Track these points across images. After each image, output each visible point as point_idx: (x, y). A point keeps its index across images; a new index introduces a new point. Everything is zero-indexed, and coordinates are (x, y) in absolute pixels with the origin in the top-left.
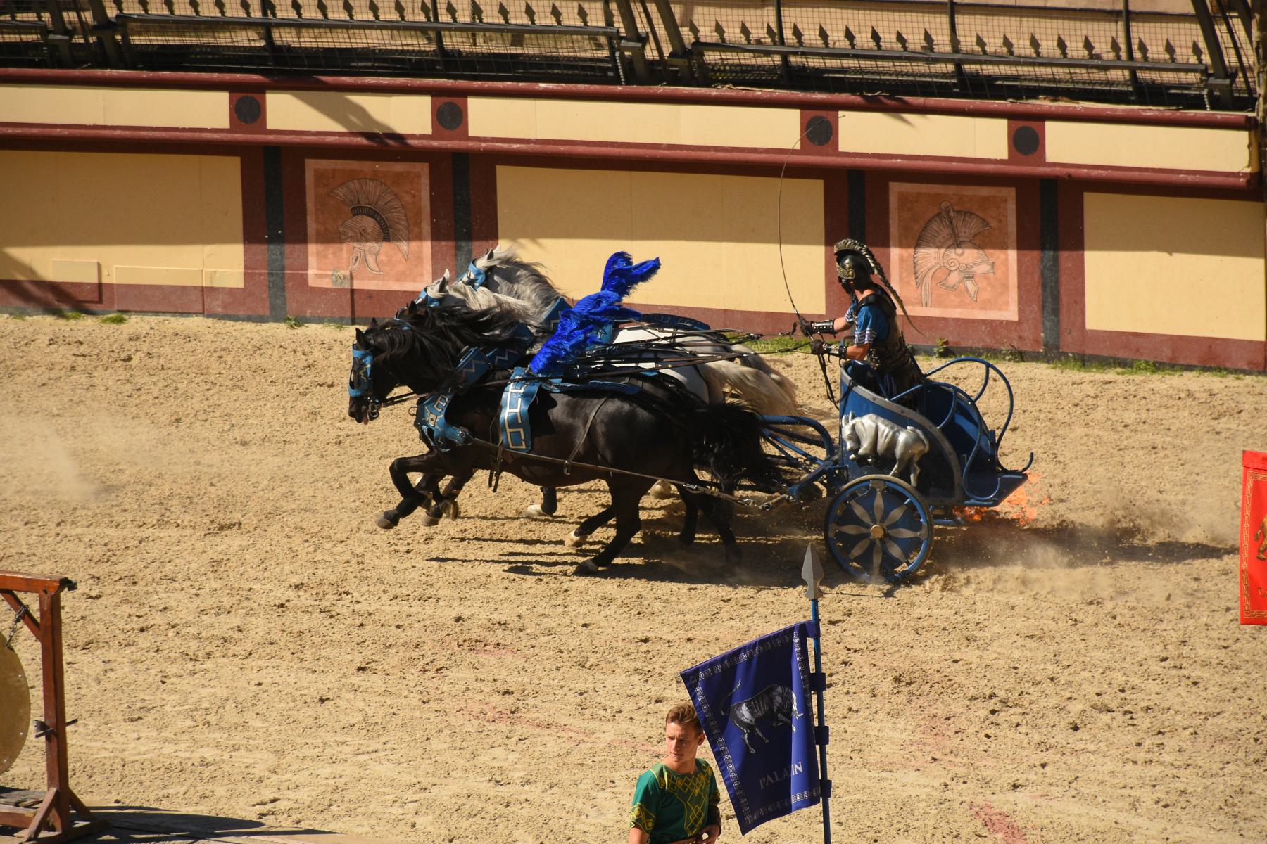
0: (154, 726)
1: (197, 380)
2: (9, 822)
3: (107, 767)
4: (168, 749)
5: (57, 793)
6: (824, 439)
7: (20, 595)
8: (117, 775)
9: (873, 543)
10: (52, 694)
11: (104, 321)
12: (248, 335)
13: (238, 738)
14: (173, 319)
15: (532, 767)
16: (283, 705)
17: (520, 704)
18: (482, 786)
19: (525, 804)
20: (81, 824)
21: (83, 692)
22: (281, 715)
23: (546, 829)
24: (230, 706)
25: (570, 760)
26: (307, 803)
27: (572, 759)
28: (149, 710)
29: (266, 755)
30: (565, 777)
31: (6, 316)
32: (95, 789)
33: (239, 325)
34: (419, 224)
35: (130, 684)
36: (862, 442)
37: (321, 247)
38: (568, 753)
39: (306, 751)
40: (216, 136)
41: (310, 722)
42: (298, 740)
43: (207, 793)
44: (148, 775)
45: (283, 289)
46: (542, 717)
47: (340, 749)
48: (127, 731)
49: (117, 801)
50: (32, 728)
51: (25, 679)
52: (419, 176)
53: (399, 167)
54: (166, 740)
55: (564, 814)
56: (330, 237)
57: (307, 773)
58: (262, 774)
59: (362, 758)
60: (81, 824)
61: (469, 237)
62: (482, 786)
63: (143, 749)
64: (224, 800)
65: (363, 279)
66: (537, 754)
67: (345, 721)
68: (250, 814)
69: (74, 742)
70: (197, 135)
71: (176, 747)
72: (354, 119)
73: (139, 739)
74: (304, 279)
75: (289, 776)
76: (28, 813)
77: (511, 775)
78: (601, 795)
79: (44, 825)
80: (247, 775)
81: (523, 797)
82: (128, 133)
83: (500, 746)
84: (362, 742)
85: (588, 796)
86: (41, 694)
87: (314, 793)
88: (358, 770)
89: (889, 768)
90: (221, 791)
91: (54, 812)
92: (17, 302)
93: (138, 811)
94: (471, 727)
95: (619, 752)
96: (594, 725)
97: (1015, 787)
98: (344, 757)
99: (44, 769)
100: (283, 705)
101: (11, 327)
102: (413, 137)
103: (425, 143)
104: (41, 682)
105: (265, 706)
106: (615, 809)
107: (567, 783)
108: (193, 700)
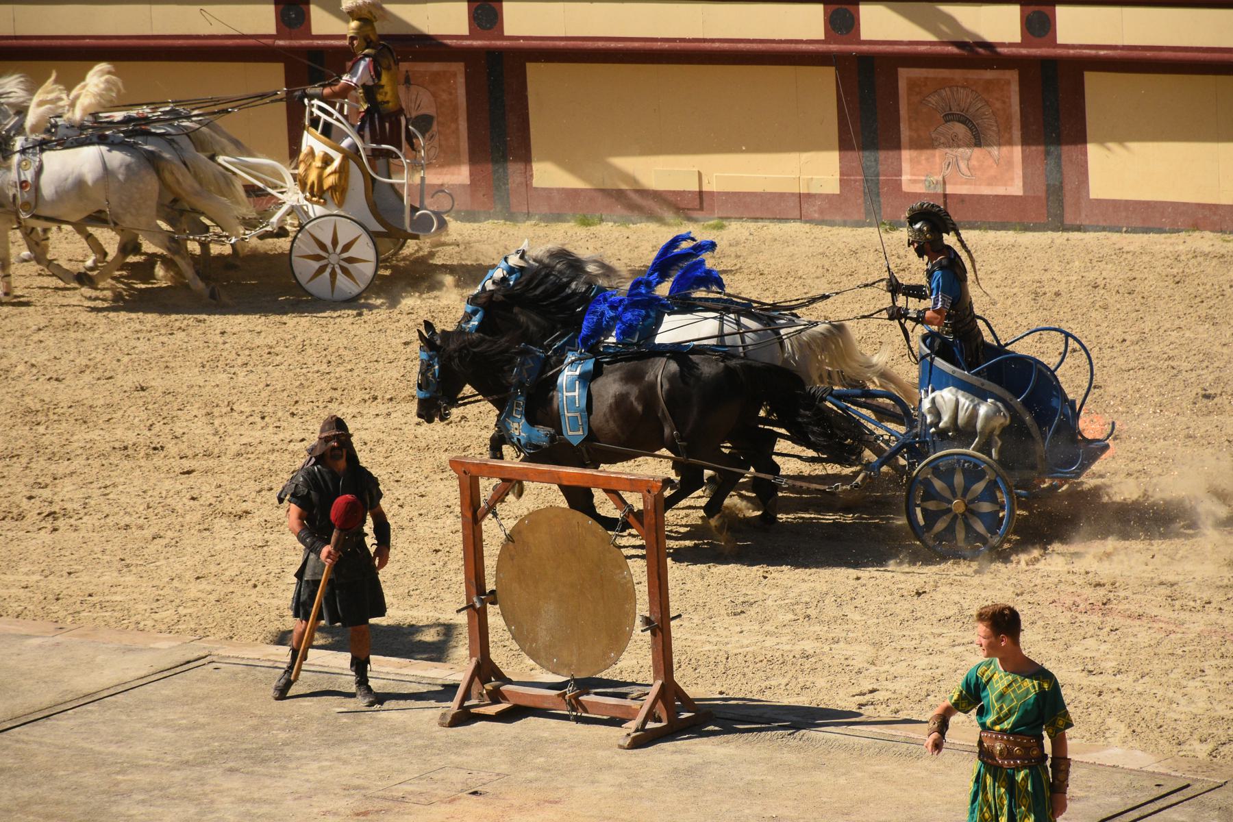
0: (757, 620)
1: (795, 284)
2: (618, 714)
3: (712, 659)
4: (770, 642)
5: (663, 685)
6: (904, 414)
7: (626, 496)
8: (721, 668)
9: (956, 516)
10: (656, 591)
11: (705, 228)
12: (845, 239)
13: (838, 632)
14: (771, 225)
15: (1124, 657)
16: (881, 598)
17: (1111, 595)
18: (1074, 676)
19: (1118, 693)
20: (686, 715)
21: (687, 587)
22: (879, 608)
23: (1138, 718)
24: (829, 600)
25: (1160, 650)
26: (905, 693)
27: (1162, 650)
28: (752, 604)
29: (864, 647)
30: (1156, 666)
31: (611, 224)
32: (699, 681)
33: (835, 230)
34: (1008, 128)
35: (733, 579)
36: (943, 416)
37: (914, 153)
38: (1158, 644)
39: (904, 643)
40: (811, 47)
41: (907, 615)
42: (896, 632)
43: (808, 684)
44: (751, 668)
45: (878, 195)
46: (1133, 608)
47: (936, 641)
48: (730, 624)
49: (721, 693)
50: (638, 624)
51: (631, 575)
52: (1008, 83)
53: (989, 75)
54: (768, 634)
55: (1155, 703)
56: (924, 143)
57: (905, 664)
58: (861, 666)
59: (958, 649)
60: (686, 715)
61: (1059, 141)
62: (1074, 676)
63: (746, 642)
64: (824, 691)
65: (955, 184)
66: (1128, 645)
67: (941, 613)
68: (849, 705)
69: (679, 636)
70: (793, 46)
71: (778, 640)
72: (944, 28)
73: (742, 632)
74: (899, 184)
75: (886, 667)
76: (635, 704)
77: (1103, 665)
78: (1191, 684)
79: (651, 716)
80: (845, 667)
81: (1114, 687)
82: (726, 46)
83: (1092, 636)
84: (959, 634)
85: (1179, 686)
86: (646, 589)
87: (912, 684)
88: (954, 661)
90: (821, 682)
91: (660, 704)
92: (619, 210)
93: (741, 702)
94: (1064, 618)
95: (1209, 642)
96: (1184, 616)
98: (940, 648)
99: (651, 662)
100: (881, 598)
101: (616, 234)
102: (1003, 45)
103: (1014, 50)
104: (645, 578)
105: (863, 600)
106: (1205, 698)
107: (1158, 672)
108: (794, 594)
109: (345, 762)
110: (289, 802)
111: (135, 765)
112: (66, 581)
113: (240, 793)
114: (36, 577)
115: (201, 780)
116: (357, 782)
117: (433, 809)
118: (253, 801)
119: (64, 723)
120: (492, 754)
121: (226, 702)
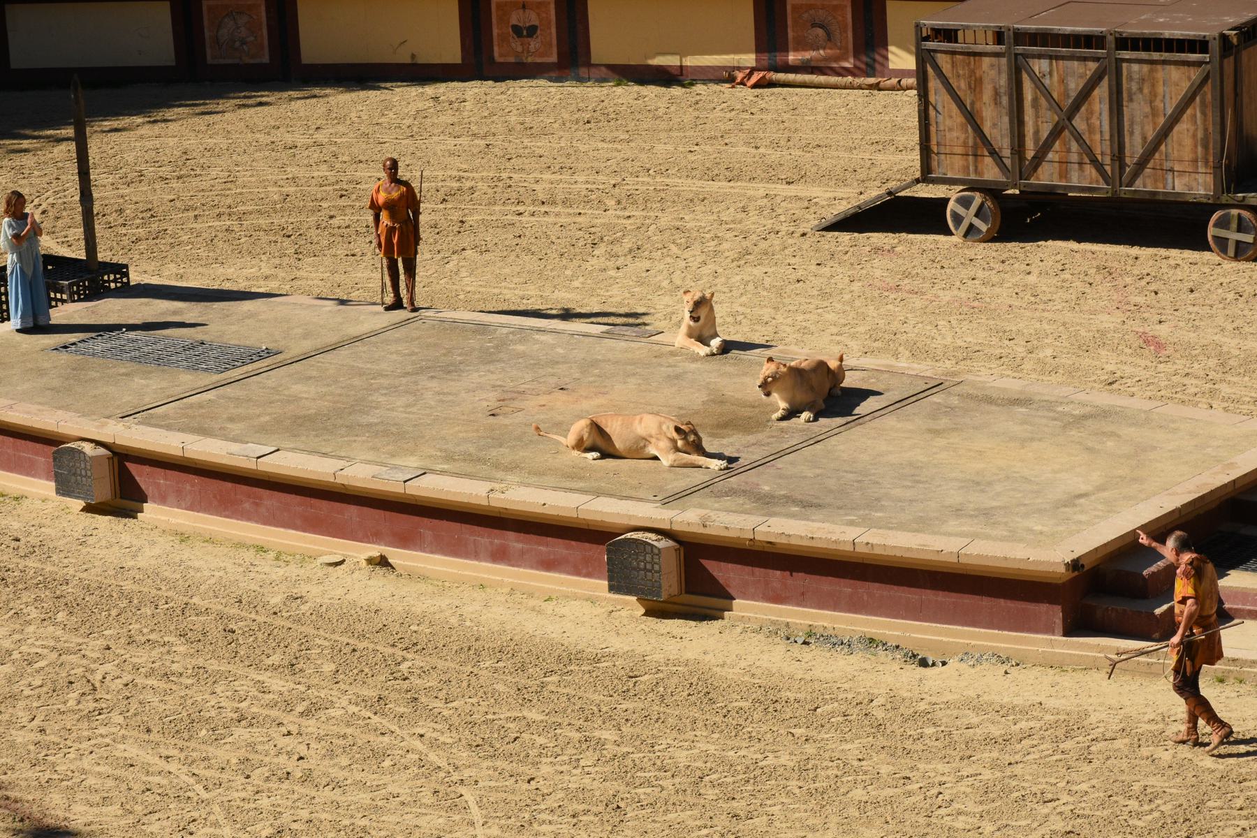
23: (915, 347)
39: (791, 307)
59: (819, 311)
89: (1094, 313)
97: (1160, 322)
109: (492, 373)
110: (463, 395)
111: (381, 374)
112: (343, 277)
113: (438, 389)
114: (328, 274)
115: (416, 383)
116: (499, 383)
117: (540, 398)
118: (444, 394)
119: (344, 352)
120: (571, 368)
121: (429, 340)
